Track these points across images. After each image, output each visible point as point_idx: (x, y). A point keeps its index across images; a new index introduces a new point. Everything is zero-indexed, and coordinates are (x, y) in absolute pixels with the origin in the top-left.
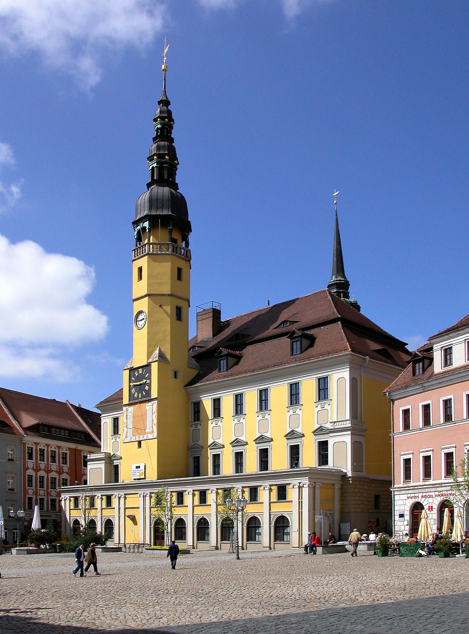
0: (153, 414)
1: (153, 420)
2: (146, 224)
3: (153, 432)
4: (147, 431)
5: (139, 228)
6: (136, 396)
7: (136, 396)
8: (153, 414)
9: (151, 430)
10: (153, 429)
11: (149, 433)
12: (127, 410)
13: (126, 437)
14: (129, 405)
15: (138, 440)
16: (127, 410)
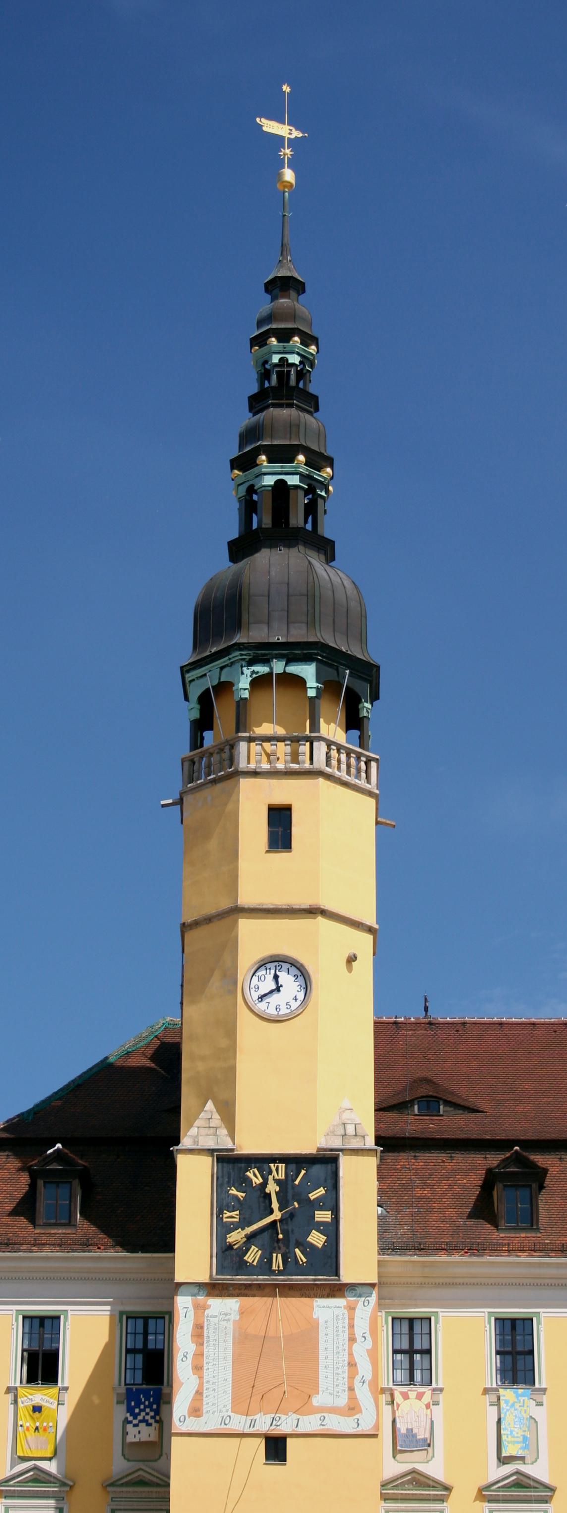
0: (352, 1339)
1: (352, 1364)
2: (308, 671)
3: (353, 1408)
4: (316, 1401)
5: (262, 669)
6: (253, 1256)
7: (253, 1256)
8: (352, 1339)
9: (343, 1400)
10: (353, 1398)
11: (333, 1410)
12: (200, 1309)
13: (196, 1411)
14: (214, 1289)
15: (264, 1424)
16: (200, 1309)
